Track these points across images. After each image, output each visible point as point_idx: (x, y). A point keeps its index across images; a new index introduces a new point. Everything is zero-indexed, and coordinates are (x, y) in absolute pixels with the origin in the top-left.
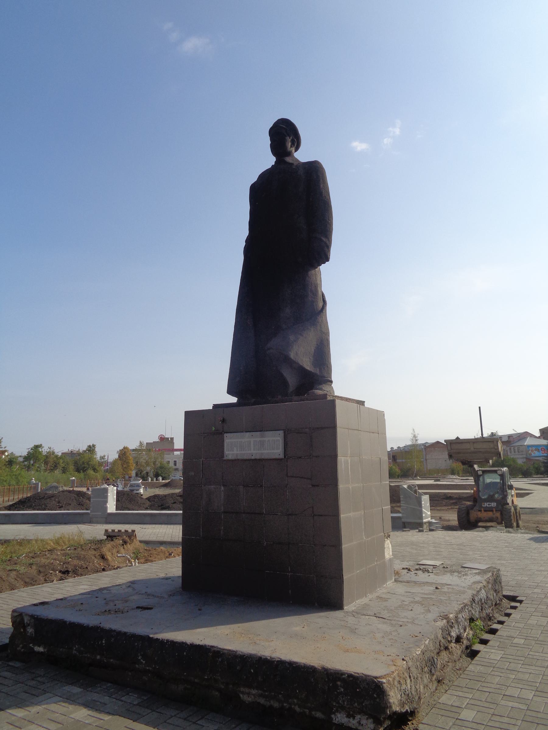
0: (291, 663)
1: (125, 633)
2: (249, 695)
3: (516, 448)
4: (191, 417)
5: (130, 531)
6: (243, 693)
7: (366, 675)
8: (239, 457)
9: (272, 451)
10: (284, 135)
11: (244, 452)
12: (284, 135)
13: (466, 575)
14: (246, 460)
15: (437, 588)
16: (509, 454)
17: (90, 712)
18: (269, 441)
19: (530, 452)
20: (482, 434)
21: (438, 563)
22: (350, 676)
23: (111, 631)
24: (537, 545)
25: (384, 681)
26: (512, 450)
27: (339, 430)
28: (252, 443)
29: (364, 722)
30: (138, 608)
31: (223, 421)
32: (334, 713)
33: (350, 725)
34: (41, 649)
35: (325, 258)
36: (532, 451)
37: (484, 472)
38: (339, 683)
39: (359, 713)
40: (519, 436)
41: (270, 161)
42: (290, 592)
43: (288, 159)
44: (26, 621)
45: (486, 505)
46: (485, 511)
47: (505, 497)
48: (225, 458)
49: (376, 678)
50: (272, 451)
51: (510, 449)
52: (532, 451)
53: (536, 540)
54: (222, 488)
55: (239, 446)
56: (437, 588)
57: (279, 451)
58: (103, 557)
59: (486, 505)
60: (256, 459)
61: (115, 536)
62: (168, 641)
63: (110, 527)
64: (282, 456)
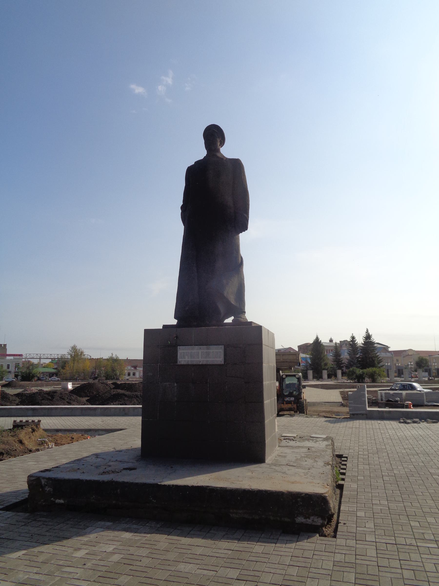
0: (266, 491)
1: (137, 484)
4: (149, 334)
5: (36, 421)
7: (316, 493)
8: (190, 363)
10: (214, 136)
12: (214, 136)
13: (317, 441)
14: (195, 365)
15: (309, 449)
17: (132, 534)
21: (295, 435)
22: (307, 494)
23: (124, 483)
24: (332, 425)
25: (327, 495)
27: (264, 346)
28: (200, 353)
29: (316, 520)
30: (124, 469)
31: (177, 337)
32: (296, 517)
33: (307, 523)
34: (62, 501)
35: (245, 228)
37: (287, 376)
38: (299, 500)
39: (313, 516)
43: (218, 155)
44: (43, 483)
45: (287, 399)
46: (286, 404)
47: (300, 393)
48: (178, 363)
49: (322, 494)
53: (329, 421)
54: (176, 385)
55: (187, 355)
56: (309, 449)
57: (221, 359)
58: (21, 442)
59: (287, 399)
60: (202, 365)
61: (25, 425)
62: (173, 485)
63: (18, 419)
64: (223, 363)
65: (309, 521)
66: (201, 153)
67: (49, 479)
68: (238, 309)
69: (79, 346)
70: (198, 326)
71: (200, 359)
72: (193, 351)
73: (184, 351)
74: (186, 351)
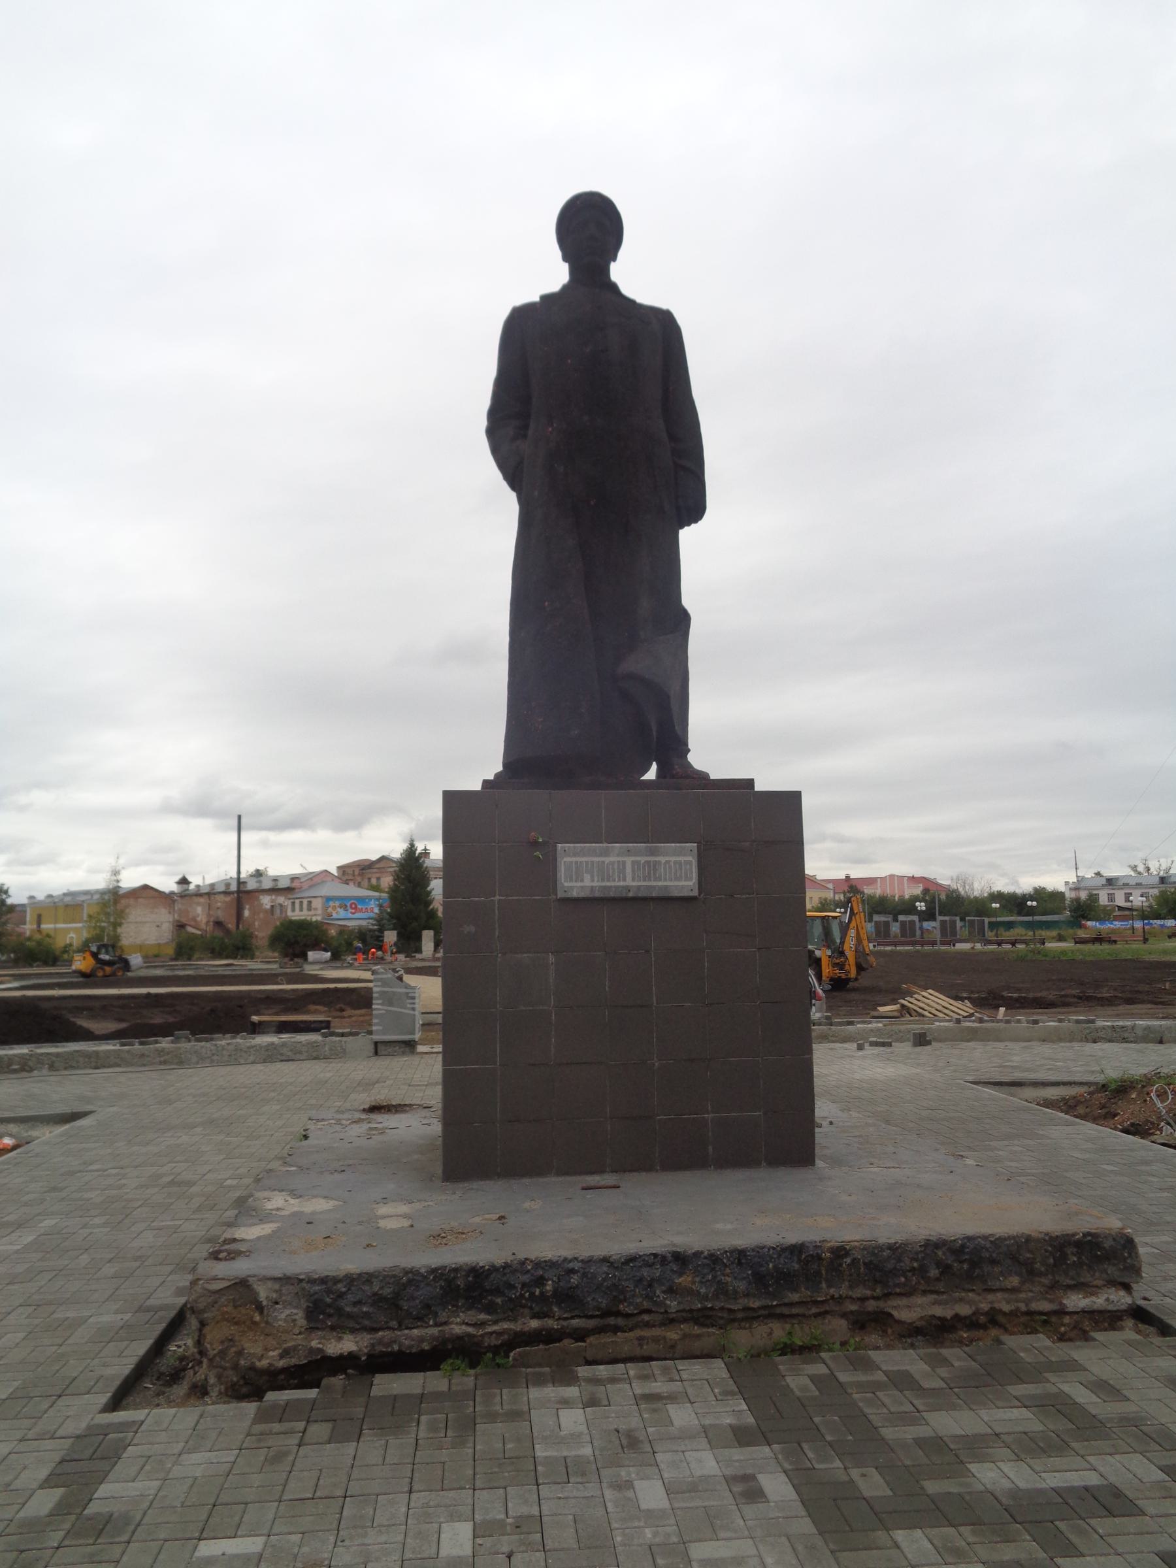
2: (909, 1310)
3: (305, 902)
6: (894, 1307)
8: (597, 894)
9: (676, 883)
10: (590, 228)
11: (608, 884)
15: (831, 1123)
18: (667, 862)
20: (239, 872)
26: (297, 906)
29: (1112, 1297)
35: (694, 510)
40: (311, 879)
41: (553, 274)
42: (710, 1148)
50: (676, 883)
51: (293, 903)
52: (334, 908)
54: (551, 958)
57: (691, 883)
65: (1099, 1301)
66: (553, 274)
67: (285, 1280)
71: (629, 882)
72: (607, 860)
73: (579, 859)
74: (584, 859)
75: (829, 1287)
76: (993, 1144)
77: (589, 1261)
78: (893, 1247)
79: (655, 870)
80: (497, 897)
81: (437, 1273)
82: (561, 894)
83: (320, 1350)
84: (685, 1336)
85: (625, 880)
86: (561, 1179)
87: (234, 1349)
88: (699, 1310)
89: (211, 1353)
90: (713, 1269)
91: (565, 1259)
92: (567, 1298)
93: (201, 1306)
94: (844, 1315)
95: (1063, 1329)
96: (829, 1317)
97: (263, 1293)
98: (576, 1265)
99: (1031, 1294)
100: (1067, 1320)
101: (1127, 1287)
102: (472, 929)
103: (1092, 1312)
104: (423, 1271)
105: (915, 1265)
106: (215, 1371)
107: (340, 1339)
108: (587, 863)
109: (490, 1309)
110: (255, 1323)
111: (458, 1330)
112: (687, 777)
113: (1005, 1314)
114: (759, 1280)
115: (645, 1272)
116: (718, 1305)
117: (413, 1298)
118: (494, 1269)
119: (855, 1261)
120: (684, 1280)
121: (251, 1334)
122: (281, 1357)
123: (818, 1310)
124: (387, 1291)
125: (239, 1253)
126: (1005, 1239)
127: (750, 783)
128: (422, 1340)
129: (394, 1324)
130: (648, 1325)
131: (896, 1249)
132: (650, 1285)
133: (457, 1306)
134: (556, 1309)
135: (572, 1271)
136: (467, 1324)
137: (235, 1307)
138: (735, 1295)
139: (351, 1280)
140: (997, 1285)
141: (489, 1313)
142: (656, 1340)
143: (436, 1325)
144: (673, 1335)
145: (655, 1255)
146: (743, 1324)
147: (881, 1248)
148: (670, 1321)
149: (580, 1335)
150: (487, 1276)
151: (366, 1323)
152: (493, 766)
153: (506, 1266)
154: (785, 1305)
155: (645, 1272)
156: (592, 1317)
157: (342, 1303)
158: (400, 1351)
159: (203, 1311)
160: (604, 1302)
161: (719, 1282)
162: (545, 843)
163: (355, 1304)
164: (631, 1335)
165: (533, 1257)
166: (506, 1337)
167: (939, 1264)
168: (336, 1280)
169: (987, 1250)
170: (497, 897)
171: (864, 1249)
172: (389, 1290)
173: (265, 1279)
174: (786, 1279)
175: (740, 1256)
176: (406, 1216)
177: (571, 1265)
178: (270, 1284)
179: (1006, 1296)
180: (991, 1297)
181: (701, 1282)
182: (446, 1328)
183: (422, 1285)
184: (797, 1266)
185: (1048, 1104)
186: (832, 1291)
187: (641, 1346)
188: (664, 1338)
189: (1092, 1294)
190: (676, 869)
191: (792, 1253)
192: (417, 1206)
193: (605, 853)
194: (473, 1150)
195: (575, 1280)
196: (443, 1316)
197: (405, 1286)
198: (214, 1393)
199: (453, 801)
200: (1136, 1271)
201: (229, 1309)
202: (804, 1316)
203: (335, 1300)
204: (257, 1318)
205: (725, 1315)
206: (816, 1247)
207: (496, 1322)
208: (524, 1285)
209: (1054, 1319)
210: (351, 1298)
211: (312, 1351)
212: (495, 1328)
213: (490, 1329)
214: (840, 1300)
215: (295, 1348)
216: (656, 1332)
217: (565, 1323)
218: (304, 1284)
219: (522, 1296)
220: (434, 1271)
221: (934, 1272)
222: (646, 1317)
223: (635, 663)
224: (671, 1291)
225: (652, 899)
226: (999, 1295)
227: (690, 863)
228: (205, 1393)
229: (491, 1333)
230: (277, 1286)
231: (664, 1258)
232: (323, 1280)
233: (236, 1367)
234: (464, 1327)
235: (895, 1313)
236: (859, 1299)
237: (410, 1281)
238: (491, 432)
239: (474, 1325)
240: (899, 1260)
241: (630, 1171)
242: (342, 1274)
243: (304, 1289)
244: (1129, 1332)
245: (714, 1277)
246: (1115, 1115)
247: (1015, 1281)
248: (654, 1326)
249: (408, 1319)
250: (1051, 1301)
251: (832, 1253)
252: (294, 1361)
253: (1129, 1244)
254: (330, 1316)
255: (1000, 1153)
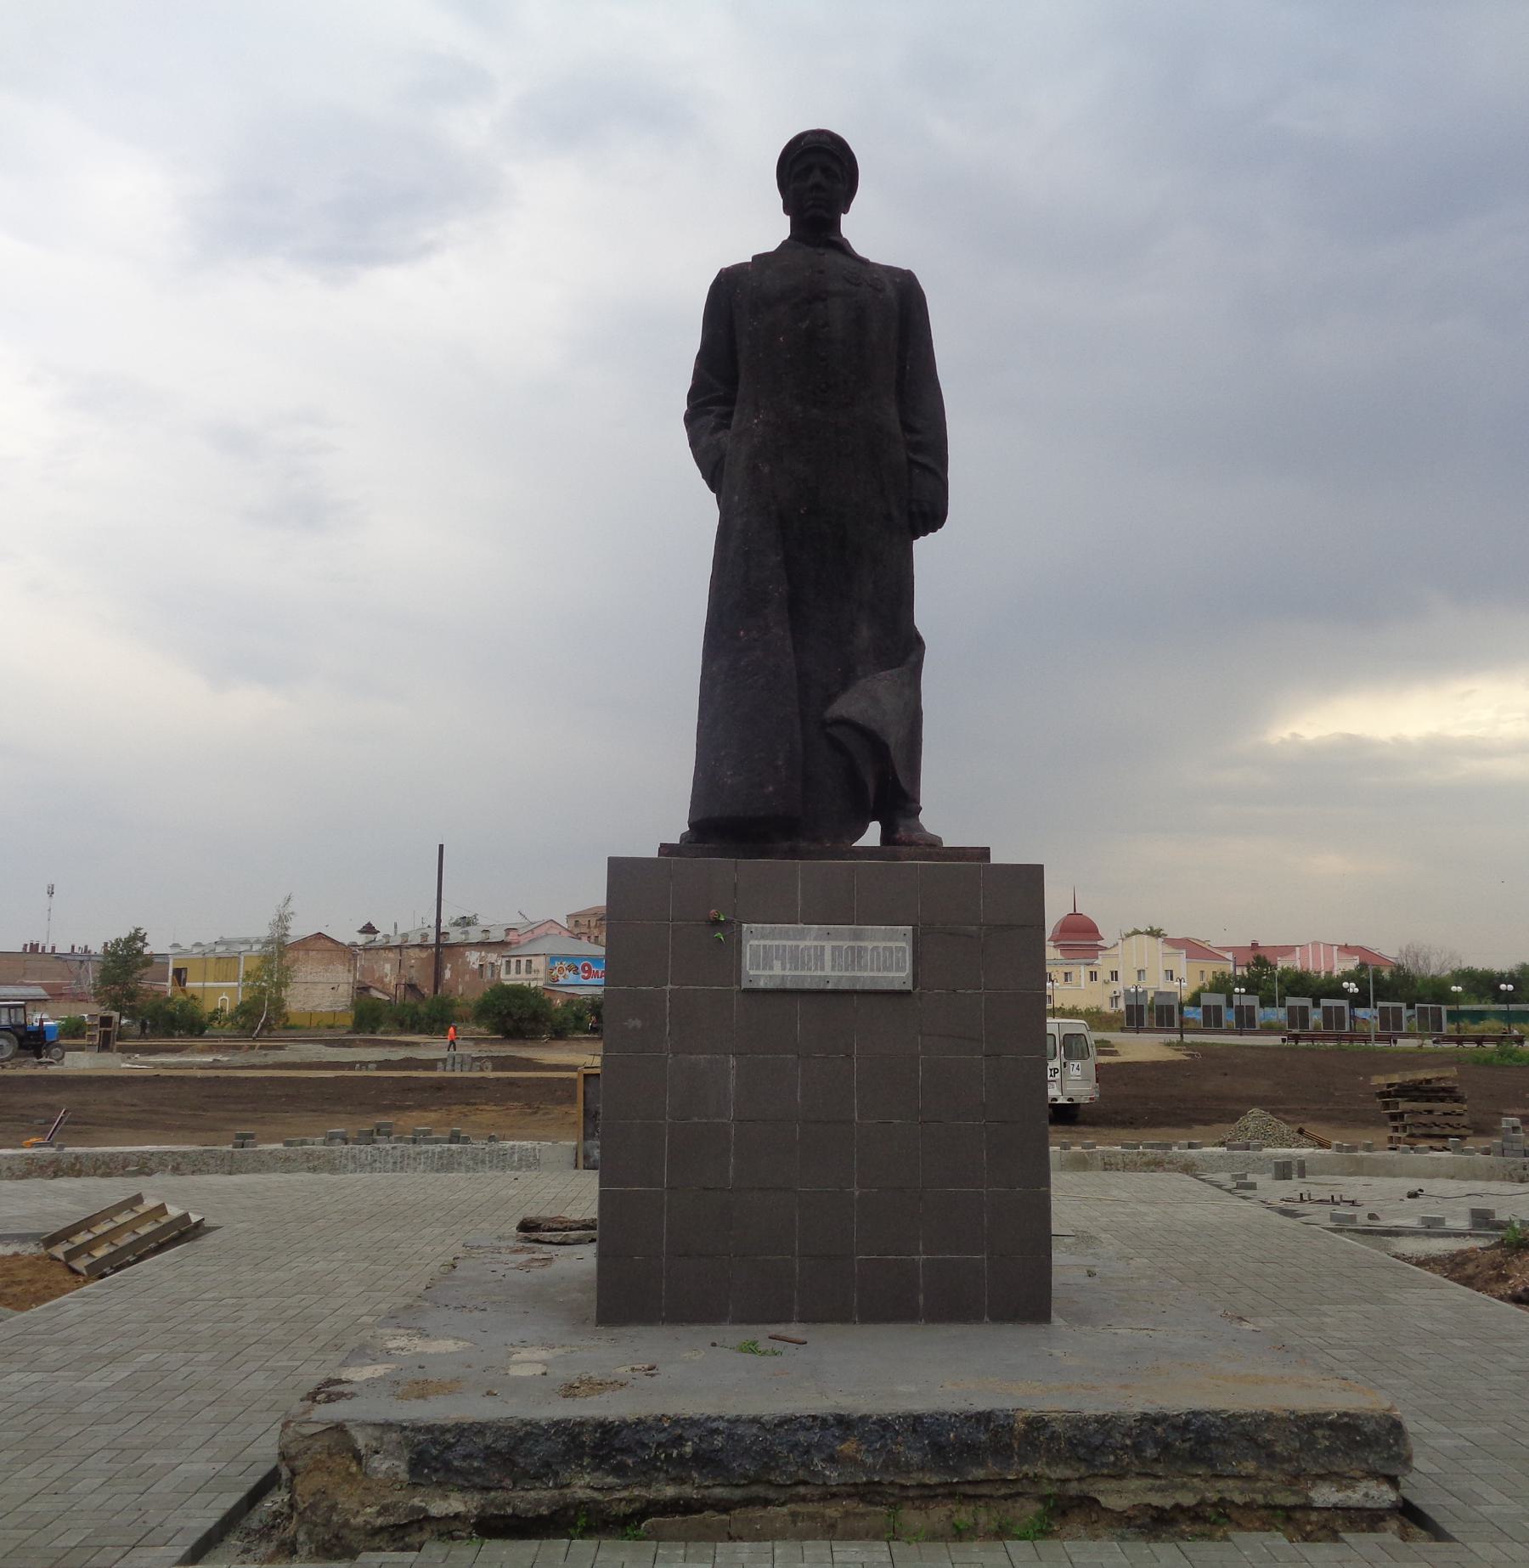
8: (789, 986)
9: (885, 974)
16: (503, 976)
19: (555, 972)
29: (1373, 1492)
35: (932, 516)
36: (561, 970)
41: (766, 227)
42: (921, 1297)
50: (885, 974)
54: (732, 1061)
67: (387, 1426)
68: (895, 798)
69: (1268, 939)
70: (793, 854)
71: (828, 972)
72: (802, 944)
73: (768, 942)
74: (777, 943)
75: (1021, 1464)
76: (1324, 1308)
77: (736, 1421)
78: (1101, 1421)
79: (860, 957)
80: (669, 987)
81: (560, 1427)
82: (745, 985)
83: (424, 1510)
84: (847, 1514)
85: (822, 969)
86: (737, 1327)
87: (326, 1503)
88: (865, 1484)
89: (302, 1506)
90: (883, 1437)
91: (709, 1418)
92: (706, 1461)
93: (293, 1452)
94: (1044, 1499)
95: (1308, 1528)
96: (1022, 1500)
97: (361, 1440)
98: (722, 1425)
99: (1270, 1484)
100: (1314, 1517)
101: (1393, 1481)
102: (638, 1023)
103: (1348, 1509)
104: (543, 1423)
105: (1128, 1442)
106: (304, 1528)
107: (446, 1497)
108: (777, 947)
109: (620, 1470)
110: (351, 1474)
111: (582, 1494)
112: (911, 844)
113: (1238, 1506)
114: (938, 1449)
115: (801, 1436)
116: (887, 1478)
117: (529, 1454)
118: (624, 1424)
119: (1054, 1437)
120: (847, 1447)
121: (346, 1487)
122: (379, 1514)
123: (1008, 1491)
124: (502, 1444)
125: (341, 1395)
126: (1241, 1417)
127: (984, 853)
128: (539, 1503)
129: (508, 1483)
130: (803, 1499)
131: (1105, 1423)
132: (807, 1452)
133: (581, 1465)
134: (695, 1475)
135: (716, 1431)
136: (592, 1488)
137: (330, 1455)
138: (907, 1469)
139: (463, 1431)
140: (1229, 1470)
141: (618, 1477)
142: (812, 1517)
143: (556, 1486)
144: (832, 1511)
145: (814, 1418)
146: (917, 1503)
147: (1086, 1421)
148: (830, 1496)
149: (724, 1506)
150: (617, 1433)
151: (477, 1480)
152: (675, 826)
153: (639, 1422)
154: (969, 1482)
155: (801, 1436)
156: (737, 1486)
157: (449, 1455)
158: (514, 1516)
159: (294, 1458)
160: (751, 1468)
161: (890, 1452)
162: (728, 922)
163: (465, 1457)
164: (785, 1510)
165: (671, 1414)
166: (637, 1505)
167: (1157, 1442)
168: (444, 1430)
169: (1217, 1428)
170: (669, 987)
171: (1067, 1421)
172: (504, 1444)
173: (364, 1425)
174: (970, 1451)
175: (916, 1423)
176: (544, 1363)
177: (715, 1425)
178: (369, 1430)
179: (1239, 1483)
180: (1220, 1485)
181: (867, 1451)
182: (566, 1491)
183: (542, 1439)
184: (983, 1438)
185: (1424, 1262)
186: (1025, 1468)
187: (794, 1523)
188: (823, 1516)
189: (1347, 1487)
190: (882, 957)
191: (978, 1421)
192: (559, 1351)
193: (802, 936)
194: (633, 1289)
195: (718, 1441)
196: (565, 1477)
197: (522, 1440)
198: (304, 1551)
199: (620, 869)
200: (1406, 1461)
201: (324, 1456)
202: (991, 1497)
203: (442, 1452)
204: (354, 1469)
205: (896, 1491)
206: (1008, 1416)
207: (626, 1487)
208: (659, 1445)
209: (1298, 1515)
210: (460, 1450)
211: (414, 1510)
212: (624, 1494)
213: (618, 1495)
214: (1036, 1480)
215: (395, 1505)
216: (811, 1508)
217: (706, 1492)
218: (407, 1433)
219: (657, 1457)
220: (557, 1423)
221: (1150, 1452)
222: (802, 1490)
223: (849, 706)
224: (832, 1459)
225: (856, 992)
226: (1231, 1483)
227: (903, 949)
228: (295, 1552)
229: (621, 1500)
230: (377, 1433)
231: (824, 1420)
232: (429, 1429)
233: (328, 1523)
234: (588, 1491)
235: (1101, 1499)
236: (1058, 1480)
237: (527, 1434)
238: (689, 420)
239: (600, 1490)
240: (1109, 1435)
241: (822, 1321)
242: (450, 1423)
243: (406, 1438)
244: (1389, 1535)
245: (883, 1446)
246: (1509, 1278)
247: (1250, 1467)
248: (812, 1501)
249: (523, 1477)
250: (1294, 1493)
251: (1028, 1424)
252: (392, 1520)
253: (1396, 1427)
254: (436, 1471)
255: (1327, 1320)
